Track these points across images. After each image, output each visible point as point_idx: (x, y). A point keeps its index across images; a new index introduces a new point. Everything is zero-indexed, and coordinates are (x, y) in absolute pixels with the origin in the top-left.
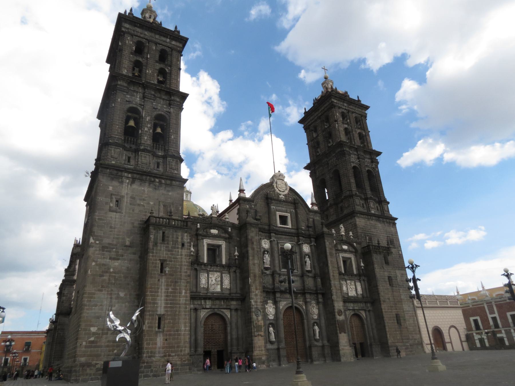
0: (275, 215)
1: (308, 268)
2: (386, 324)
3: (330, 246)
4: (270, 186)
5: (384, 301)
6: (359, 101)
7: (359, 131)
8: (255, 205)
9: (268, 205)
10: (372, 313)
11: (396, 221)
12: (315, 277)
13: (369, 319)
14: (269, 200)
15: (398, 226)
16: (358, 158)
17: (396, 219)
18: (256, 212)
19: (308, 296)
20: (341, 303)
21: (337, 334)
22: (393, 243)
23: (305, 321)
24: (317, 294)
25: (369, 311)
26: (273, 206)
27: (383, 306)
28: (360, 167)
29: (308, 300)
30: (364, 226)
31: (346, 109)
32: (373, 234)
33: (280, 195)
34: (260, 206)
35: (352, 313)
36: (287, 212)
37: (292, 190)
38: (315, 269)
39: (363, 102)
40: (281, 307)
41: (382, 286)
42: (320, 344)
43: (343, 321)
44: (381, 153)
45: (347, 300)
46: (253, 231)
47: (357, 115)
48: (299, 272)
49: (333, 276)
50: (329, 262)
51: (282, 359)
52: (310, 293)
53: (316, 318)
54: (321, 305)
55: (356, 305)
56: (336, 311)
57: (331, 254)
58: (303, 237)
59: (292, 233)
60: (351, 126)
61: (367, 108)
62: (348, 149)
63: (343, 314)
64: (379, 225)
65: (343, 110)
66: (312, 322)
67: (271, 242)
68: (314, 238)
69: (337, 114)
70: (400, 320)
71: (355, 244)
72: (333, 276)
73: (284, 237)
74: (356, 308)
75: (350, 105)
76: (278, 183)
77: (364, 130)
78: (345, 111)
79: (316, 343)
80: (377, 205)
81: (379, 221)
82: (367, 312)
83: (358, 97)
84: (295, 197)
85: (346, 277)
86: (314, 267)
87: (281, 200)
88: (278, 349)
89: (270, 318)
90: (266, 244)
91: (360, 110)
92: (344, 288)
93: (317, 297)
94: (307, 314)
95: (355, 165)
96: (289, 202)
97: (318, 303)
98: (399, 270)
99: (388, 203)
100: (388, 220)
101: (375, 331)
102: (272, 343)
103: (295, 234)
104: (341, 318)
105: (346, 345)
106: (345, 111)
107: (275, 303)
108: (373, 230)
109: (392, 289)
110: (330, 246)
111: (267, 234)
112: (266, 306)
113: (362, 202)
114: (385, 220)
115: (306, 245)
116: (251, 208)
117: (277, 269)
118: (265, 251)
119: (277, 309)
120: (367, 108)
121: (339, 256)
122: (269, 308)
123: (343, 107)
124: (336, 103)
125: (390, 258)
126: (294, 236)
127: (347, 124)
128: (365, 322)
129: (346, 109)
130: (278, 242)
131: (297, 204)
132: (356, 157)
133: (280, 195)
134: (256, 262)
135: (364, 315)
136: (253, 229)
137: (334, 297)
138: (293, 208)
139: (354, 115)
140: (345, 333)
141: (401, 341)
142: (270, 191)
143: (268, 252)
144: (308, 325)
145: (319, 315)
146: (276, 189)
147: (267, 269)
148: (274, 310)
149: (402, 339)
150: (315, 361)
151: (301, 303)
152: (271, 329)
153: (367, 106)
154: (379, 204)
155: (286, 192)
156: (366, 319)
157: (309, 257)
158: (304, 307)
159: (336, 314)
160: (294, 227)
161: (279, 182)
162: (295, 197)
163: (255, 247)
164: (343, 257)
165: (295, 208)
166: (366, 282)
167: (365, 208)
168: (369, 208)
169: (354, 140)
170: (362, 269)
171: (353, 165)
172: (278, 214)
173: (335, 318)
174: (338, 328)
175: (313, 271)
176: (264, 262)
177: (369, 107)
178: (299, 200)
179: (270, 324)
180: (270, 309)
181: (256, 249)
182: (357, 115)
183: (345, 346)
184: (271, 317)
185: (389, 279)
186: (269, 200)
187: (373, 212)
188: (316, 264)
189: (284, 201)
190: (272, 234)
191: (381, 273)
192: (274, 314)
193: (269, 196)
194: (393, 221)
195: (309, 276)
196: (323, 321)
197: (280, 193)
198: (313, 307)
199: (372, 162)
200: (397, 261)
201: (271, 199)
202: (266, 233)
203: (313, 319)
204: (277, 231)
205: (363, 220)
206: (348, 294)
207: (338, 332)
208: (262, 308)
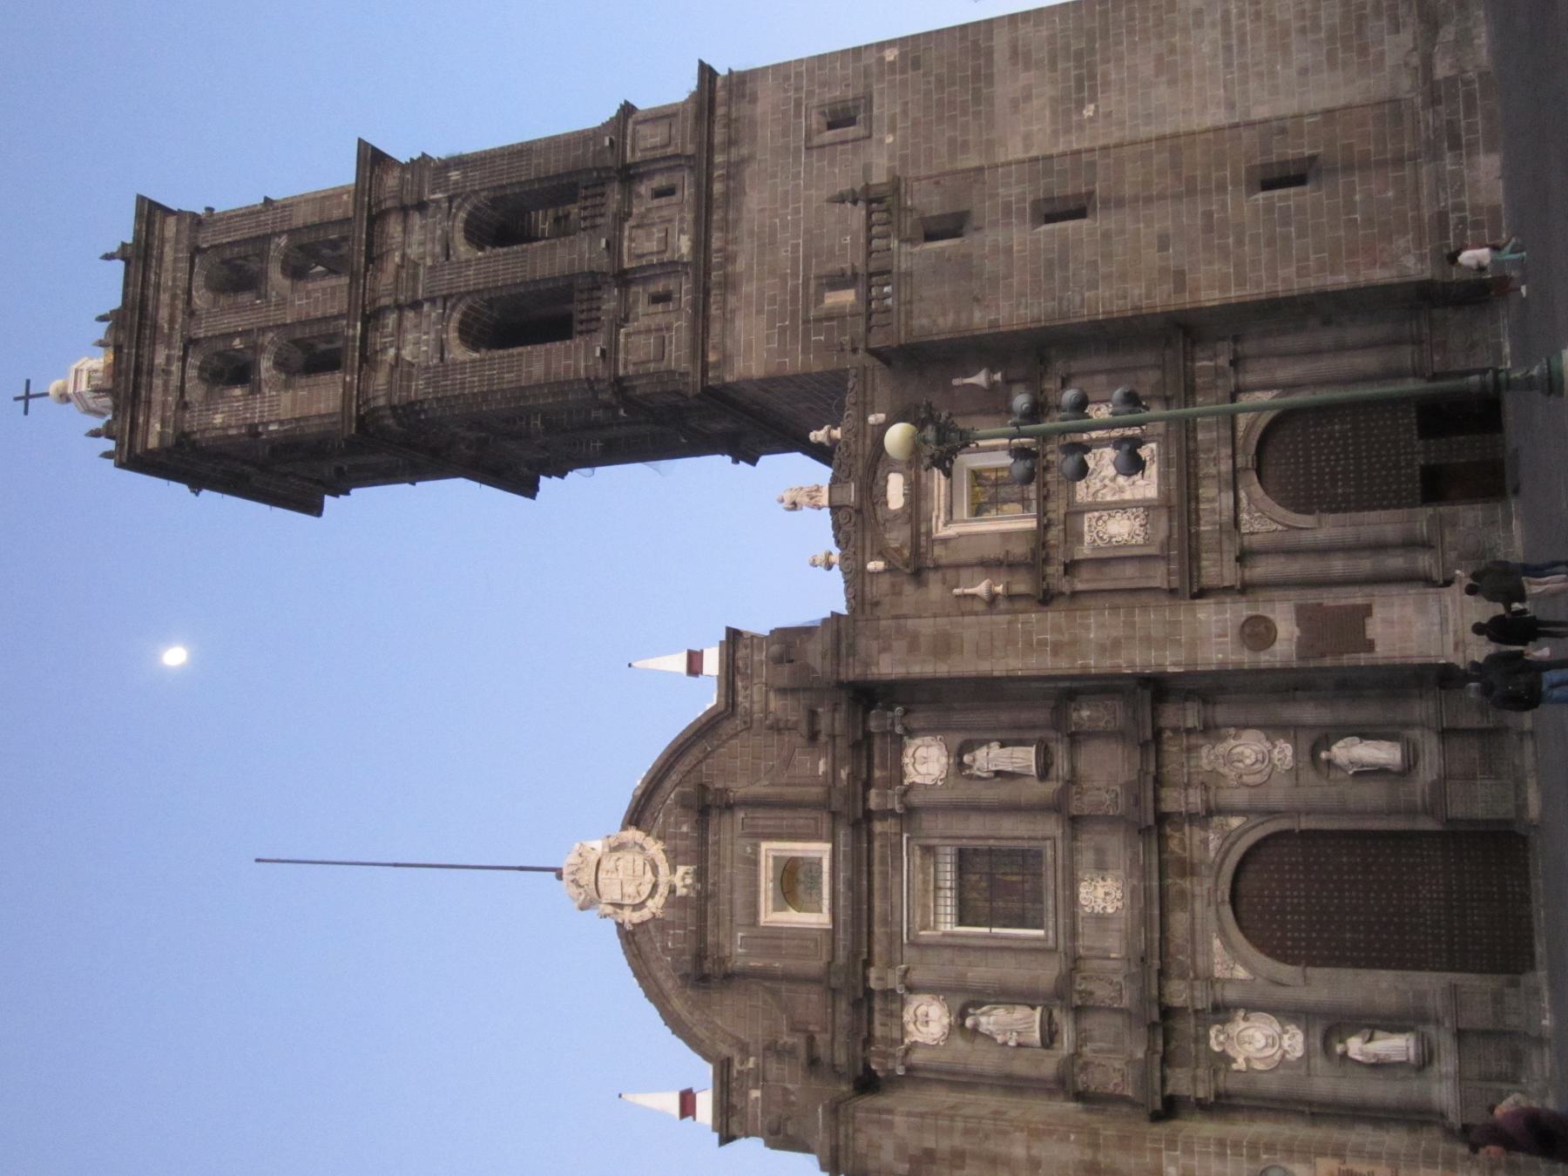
0: (777, 935)
1: (1023, 758)
2: (1313, 283)
3: (900, 645)
4: (631, 938)
5: (1180, 278)
6: (124, 254)
7: (276, 276)
8: (744, 1050)
9: (729, 977)
10: (1249, 347)
11: (722, 70)
12: (1075, 739)
13: (1285, 373)
14: (708, 966)
15: (740, 66)
16: (416, 305)
17: (706, 73)
18: (774, 1049)
19: (1173, 800)
20: (1201, 616)
21: (1375, 668)
22: (840, 94)
23: (1306, 824)
24: (1158, 734)
25: (1234, 363)
26: (732, 937)
27: (1210, 297)
28: (461, 296)
29: (1195, 799)
30: (771, 326)
31: (184, 359)
32: (807, 258)
33: (672, 890)
34: (738, 1016)
35: (1257, 489)
36: (754, 862)
37: (638, 816)
38: (1034, 727)
39: (129, 241)
40: (1241, 973)
41: (1093, 285)
42: (1430, 746)
43: (1304, 615)
44: (360, 141)
45: (1183, 561)
46: (870, 1145)
47: (199, 281)
48: (1051, 827)
49: (1057, 649)
50: (985, 667)
51: (1512, 1021)
52: (1159, 782)
53: (1289, 750)
54: (1221, 714)
55: (1207, 469)
56: (1245, 658)
57: (944, 645)
58: (868, 785)
59: (855, 848)
60: (263, 330)
61: (150, 213)
62: (381, 379)
63: (1263, 610)
64: (754, 201)
65: (192, 373)
66: (1309, 776)
67: (911, 989)
68: (865, 722)
69: (218, 419)
70: (1283, 164)
71: (872, 419)
72: (1057, 649)
73: (877, 903)
74: (1226, 467)
75: (155, 327)
76: (617, 897)
77: (267, 238)
78: (194, 360)
79: (1428, 770)
80: (644, 189)
81: (733, 196)
82: (1250, 378)
83: (108, 257)
84: (670, 794)
85: (1057, 509)
86: (1017, 727)
87: (699, 893)
88: (1460, 1035)
89: (1299, 1053)
90: (927, 1022)
91: (168, 250)
92: (1121, 528)
93: (1176, 730)
94: (1272, 813)
95: (453, 335)
96: (703, 841)
97: (1210, 730)
98: (990, 80)
99: (627, 110)
100: (719, 138)
101: (1353, 334)
102: (1426, 1060)
103: (856, 839)
104: (1287, 629)
105: (1434, 609)
106: (194, 360)
107: (1222, 1011)
108: (784, 253)
109: (1106, 203)
110: (900, 645)
111: (878, 1004)
112: (1240, 1064)
113: (642, 307)
114: (719, 159)
115: (906, 760)
116: (760, 1077)
117: (1047, 973)
118: (959, 1027)
119: (1251, 1008)
120: (150, 213)
121: (945, 541)
122: (1250, 1049)
123: (175, 380)
124: (163, 423)
125: (928, 201)
126: (870, 842)
127: (257, 349)
128: (1300, 398)
129: (184, 359)
130: (912, 944)
131: (703, 788)
132: (410, 314)
133: (672, 890)
134: (1019, 1151)
135: (1264, 397)
136: (861, 1142)
137: (1170, 661)
138: (727, 818)
139: (201, 298)
140: (1367, 611)
141: (1407, 171)
142: (665, 949)
143: (963, 1014)
144: (1327, 812)
145: (1275, 729)
146: (645, 914)
147: (1050, 1036)
148: (1253, 1016)
149: (1398, 162)
150: (1522, 807)
151: (1214, 841)
152: (1355, 1046)
153: (139, 216)
154: (641, 177)
155: (655, 849)
156: (1289, 387)
157: (968, 746)
158: (1235, 822)
159: (1265, 659)
160: (825, 828)
161: (611, 892)
162: (670, 794)
163: (944, 1145)
164: (950, 519)
165: (730, 807)
166: (1075, 366)
167: (672, 285)
168: (671, 267)
169: (325, 319)
170: (1008, 382)
171: (458, 352)
172: (771, 916)
173: (1286, 670)
174: (1347, 660)
175: (1038, 734)
176: (1019, 1045)
177: (141, 200)
178: (682, 767)
179: (1327, 1048)
180: (1258, 1044)
181: (958, 1141)
182: (199, 281)
183: (1444, 622)
184: (1294, 1042)
185: (1050, 218)
186: (708, 966)
187: (684, 244)
188: (1004, 717)
189: (701, 875)
190: (873, 984)
191: (1013, 277)
192: (1277, 1028)
193: (688, 968)
194: (721, 95)
195: (1073, 779)
196: (1309, 713)
197: (663, 889)
198: (1229, 759)
199: (421, 206)
200: (939, 80)
201: (700, 956)
202: (871, 1011)
203: (1295, 772)
204: (854, 955)
205: (739, 323)
206: (1147, 506)
207: (1363, 659)
208: (1254, 1157)
